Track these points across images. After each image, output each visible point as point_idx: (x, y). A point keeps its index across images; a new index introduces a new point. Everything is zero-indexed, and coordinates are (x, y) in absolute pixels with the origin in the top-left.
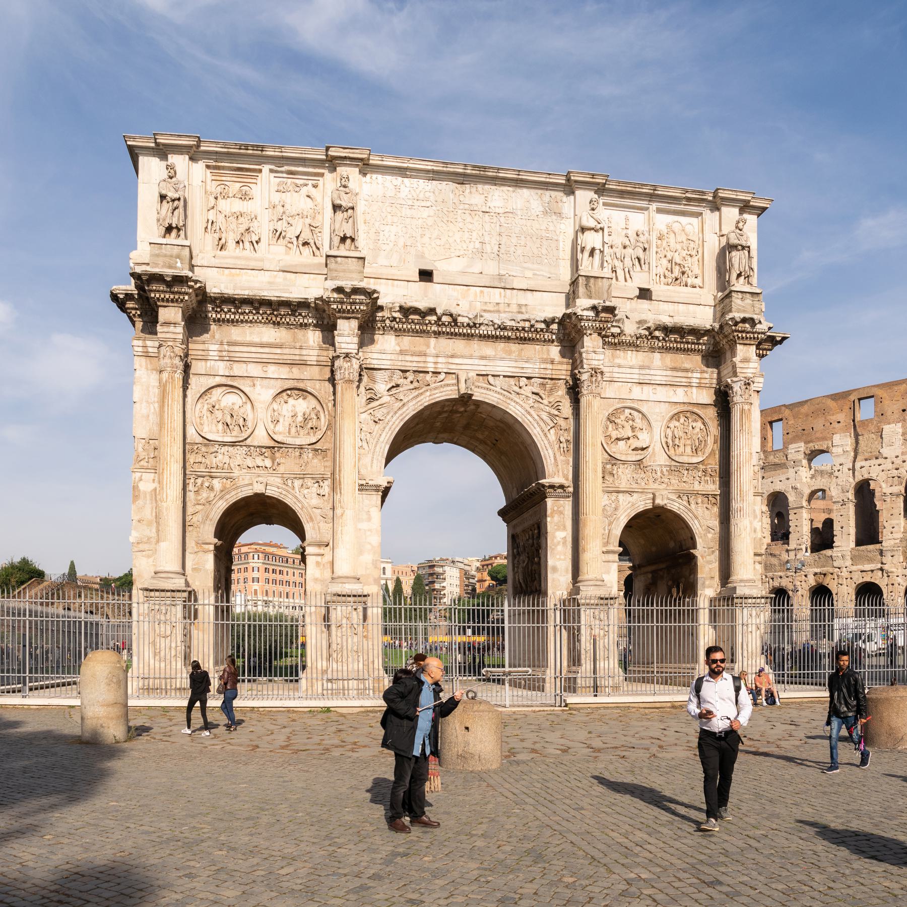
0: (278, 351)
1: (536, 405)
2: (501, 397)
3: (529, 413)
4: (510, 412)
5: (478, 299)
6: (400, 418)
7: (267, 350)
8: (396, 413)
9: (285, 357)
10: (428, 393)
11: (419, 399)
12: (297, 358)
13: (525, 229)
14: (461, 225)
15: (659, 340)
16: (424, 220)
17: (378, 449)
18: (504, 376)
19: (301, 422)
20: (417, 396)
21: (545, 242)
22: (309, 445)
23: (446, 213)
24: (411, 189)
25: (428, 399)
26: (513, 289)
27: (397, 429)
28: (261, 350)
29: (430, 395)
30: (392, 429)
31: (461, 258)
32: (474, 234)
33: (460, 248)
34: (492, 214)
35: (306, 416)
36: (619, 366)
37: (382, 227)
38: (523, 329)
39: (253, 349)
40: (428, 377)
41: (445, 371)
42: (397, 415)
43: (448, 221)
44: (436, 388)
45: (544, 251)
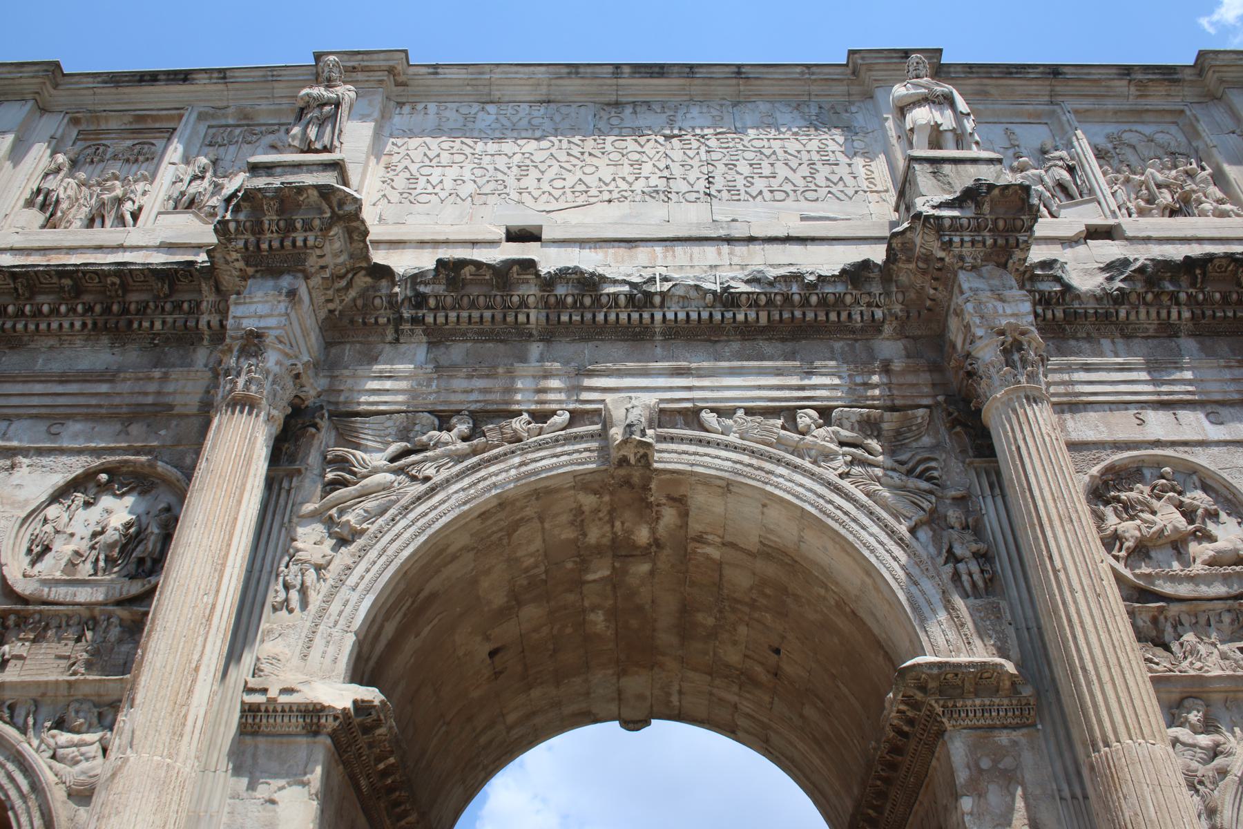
0: (104, 388)
1: (856, 470)
2: (746, 459)
3: (837, 490)
4: (777, 492)
5: (659, 262)
6: (419, 523)
7: (73, 388)
8: (406, 509)
9: (117, 401)
10: (517, 460)
11: (482, 473)
12: (150, 400)
13: (767, 152)
14: (615, 156)
15: (1178, 303)
16: (527, 155)
17: (335, 607)
18: (749, 412)
19: (111, 546)
20: (475, 468)
21: (824, 171)
22: (120, 603)
23: (579, 143)
24: (501, 118)
25: (513, 472)
26: (751, 240)
27: (406, 553)
28: (59, 389)
29: (523, 464)
30: (390, 552)
31: (615, 204)
32: (647, 169)
33: (611, 188)
34: (685, 137)
35: (132, 530)
36: (1087, 368)
37: (425, 171)
38: (787, 298)
39: (38, 388)
40: (518, 424)
41: (571, 406)
42: (412, 516)
43: (582, 153)
44: (540, 446)
45: (823, 183)
